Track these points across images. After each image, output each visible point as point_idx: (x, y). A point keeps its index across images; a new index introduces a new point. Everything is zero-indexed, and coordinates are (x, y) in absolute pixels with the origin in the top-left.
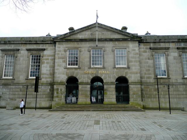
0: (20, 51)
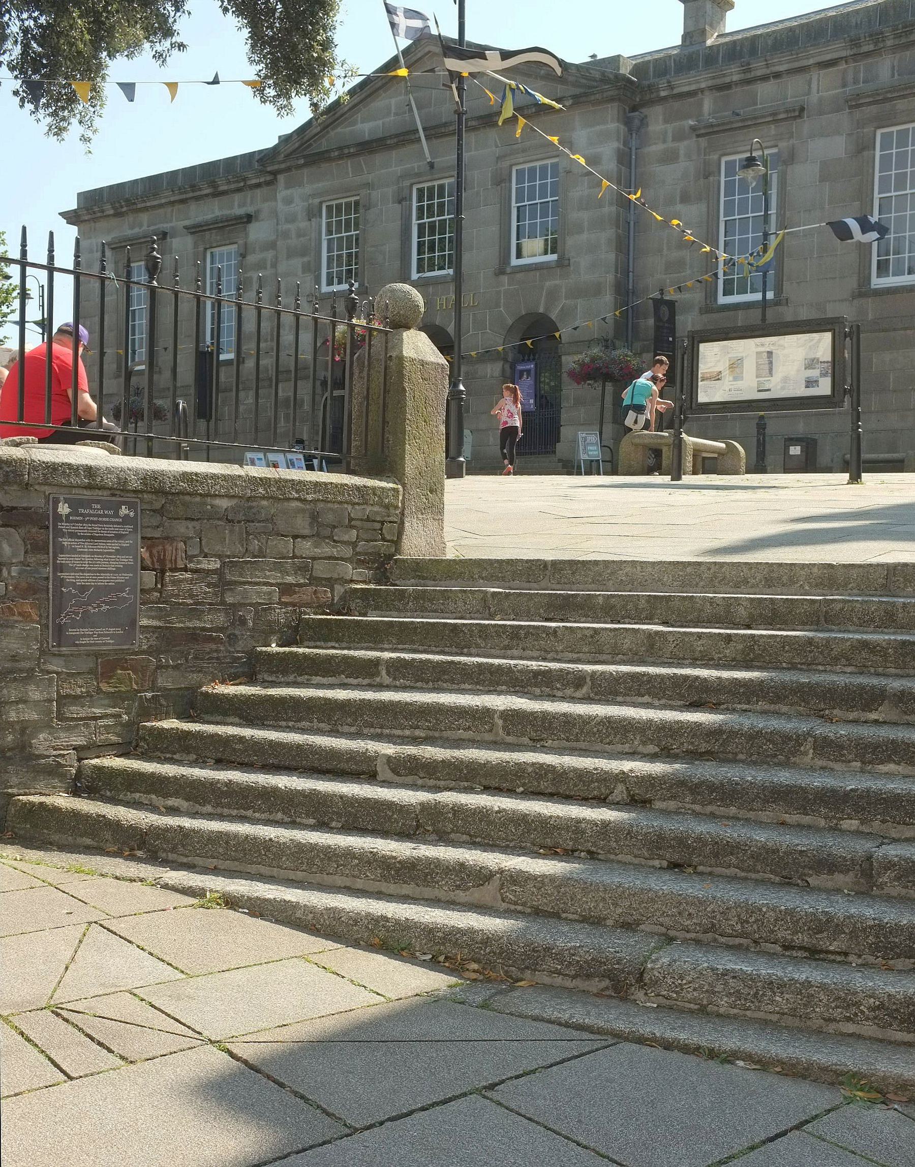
0: (168, 239)
